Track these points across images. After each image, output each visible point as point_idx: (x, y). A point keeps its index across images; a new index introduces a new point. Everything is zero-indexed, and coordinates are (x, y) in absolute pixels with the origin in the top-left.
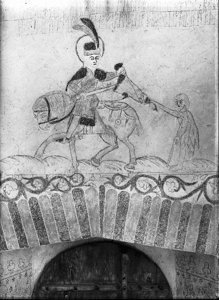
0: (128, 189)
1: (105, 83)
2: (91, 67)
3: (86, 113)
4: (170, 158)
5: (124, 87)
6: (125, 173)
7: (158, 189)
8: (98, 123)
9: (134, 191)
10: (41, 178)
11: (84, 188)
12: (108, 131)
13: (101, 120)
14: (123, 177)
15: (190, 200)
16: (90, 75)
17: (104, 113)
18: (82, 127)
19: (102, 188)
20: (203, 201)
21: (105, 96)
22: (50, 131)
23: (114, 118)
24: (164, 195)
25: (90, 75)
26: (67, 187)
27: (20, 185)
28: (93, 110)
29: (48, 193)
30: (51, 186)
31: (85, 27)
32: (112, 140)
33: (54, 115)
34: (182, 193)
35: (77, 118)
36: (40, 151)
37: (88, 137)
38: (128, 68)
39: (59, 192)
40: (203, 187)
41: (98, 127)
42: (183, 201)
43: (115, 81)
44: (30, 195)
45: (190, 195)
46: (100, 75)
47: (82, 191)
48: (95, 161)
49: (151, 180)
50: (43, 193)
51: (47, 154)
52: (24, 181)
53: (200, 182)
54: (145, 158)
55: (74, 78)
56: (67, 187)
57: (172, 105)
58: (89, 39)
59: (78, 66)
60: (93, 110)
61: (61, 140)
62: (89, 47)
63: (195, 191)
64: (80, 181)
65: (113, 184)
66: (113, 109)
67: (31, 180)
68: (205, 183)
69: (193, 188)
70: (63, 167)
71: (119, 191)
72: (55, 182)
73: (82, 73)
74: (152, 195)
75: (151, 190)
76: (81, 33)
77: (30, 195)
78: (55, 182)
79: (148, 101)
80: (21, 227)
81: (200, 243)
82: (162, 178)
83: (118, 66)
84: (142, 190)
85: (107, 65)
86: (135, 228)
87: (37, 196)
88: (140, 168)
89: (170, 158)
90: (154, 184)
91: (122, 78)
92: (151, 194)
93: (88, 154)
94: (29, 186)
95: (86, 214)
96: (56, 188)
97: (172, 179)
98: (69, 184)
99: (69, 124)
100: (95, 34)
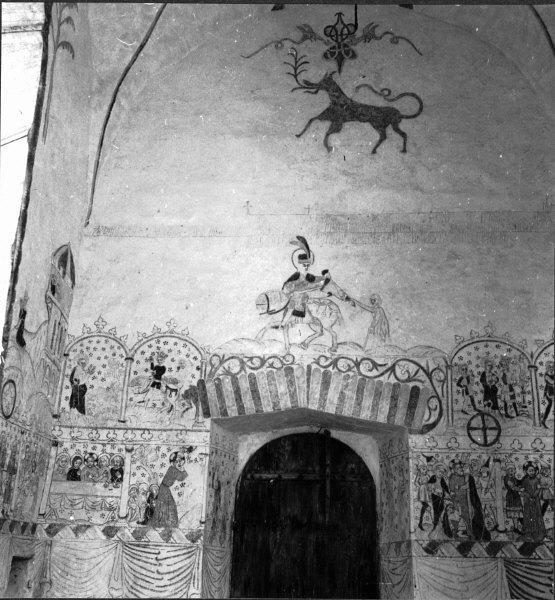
0: (330, 368)
1: (314, 285)
2: (303, 272)
3: (299, 307)
4: (366, 343)
5: (330, 288)
6: (328, 355)
7: (355, 369)
8: (307, 315)
9: (336, 370)
10: (259, 357)
11: (294, 367)
12: (315, 321)
13: (310, 313)
14: (327, 359)
15: (381, 378)
16: (302, 278)
17: (312, 307)
18: (294, 318)
19: (309, 367)
20: (393, 380)
21: (315, 294)
22: (269, 320)
23: (321, 311)
24: (361, 374)
25: (302, 278)
26: (280, 365)
27: (242, 362)
28: (304, 305)
29: (265, 370)
30: (267, 364)
31: (300, 243)
32: (318, 329)
33: (271, 308)
34: (375, 373)
35: (290, 311)
36: (260, 335)
37: (299, 326)
38: (332, 274)
39: (274, 370)
40: (392, 369)
41: (307, 318)
42: (376, 380)
43: (322, 282)
44: (249, 371)
45: (382, 374)
46: (310, 278)
47: (292, 369)
48: (304, 345)
49: (349, 362)
50: (260, 370)
51: (265, 338)
52: (245, 360)
53: (390, 365)
54: (345, 343)
55: (290, 280)
56: (280, 365)
57: (367, 302)
58: (302, 252)
59: (293, 272)
60: (304, 305)
61: (277, 327)
62: (302, 257)
63: (387, 371)
64: (291, 360)
65: (318, 364)
66: (322, 304)
67: (251, 359)
68: (394, 365)
69: (384, 369)
70: (277, 349)
71: (322, 370)
72: (271, 361)
73: (296, 277)
74: (351, 374)
75: (350, 369)
76: (296, 247)
77: (249, 371)
78: (271, 361)
79: (348, 299)
80: (240, 397)
81: (391, 415)
82: (359, 360)
83: (325, 272)
84: (342, 369)
85: (316, 271)
86: (336, 401)
87: (255, 372)
88: (340, 351)
89: (366, 343)
90: (352, 365)
91: (327, 281)
92: (349, 373)
93: (299, 340)
94: (249, 363)
95: (295, 390)
96: (271, 366)
97: (366, 361)
98: (282, 362)
99: (284, 315)
100: (308, 248)
